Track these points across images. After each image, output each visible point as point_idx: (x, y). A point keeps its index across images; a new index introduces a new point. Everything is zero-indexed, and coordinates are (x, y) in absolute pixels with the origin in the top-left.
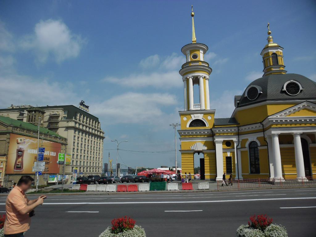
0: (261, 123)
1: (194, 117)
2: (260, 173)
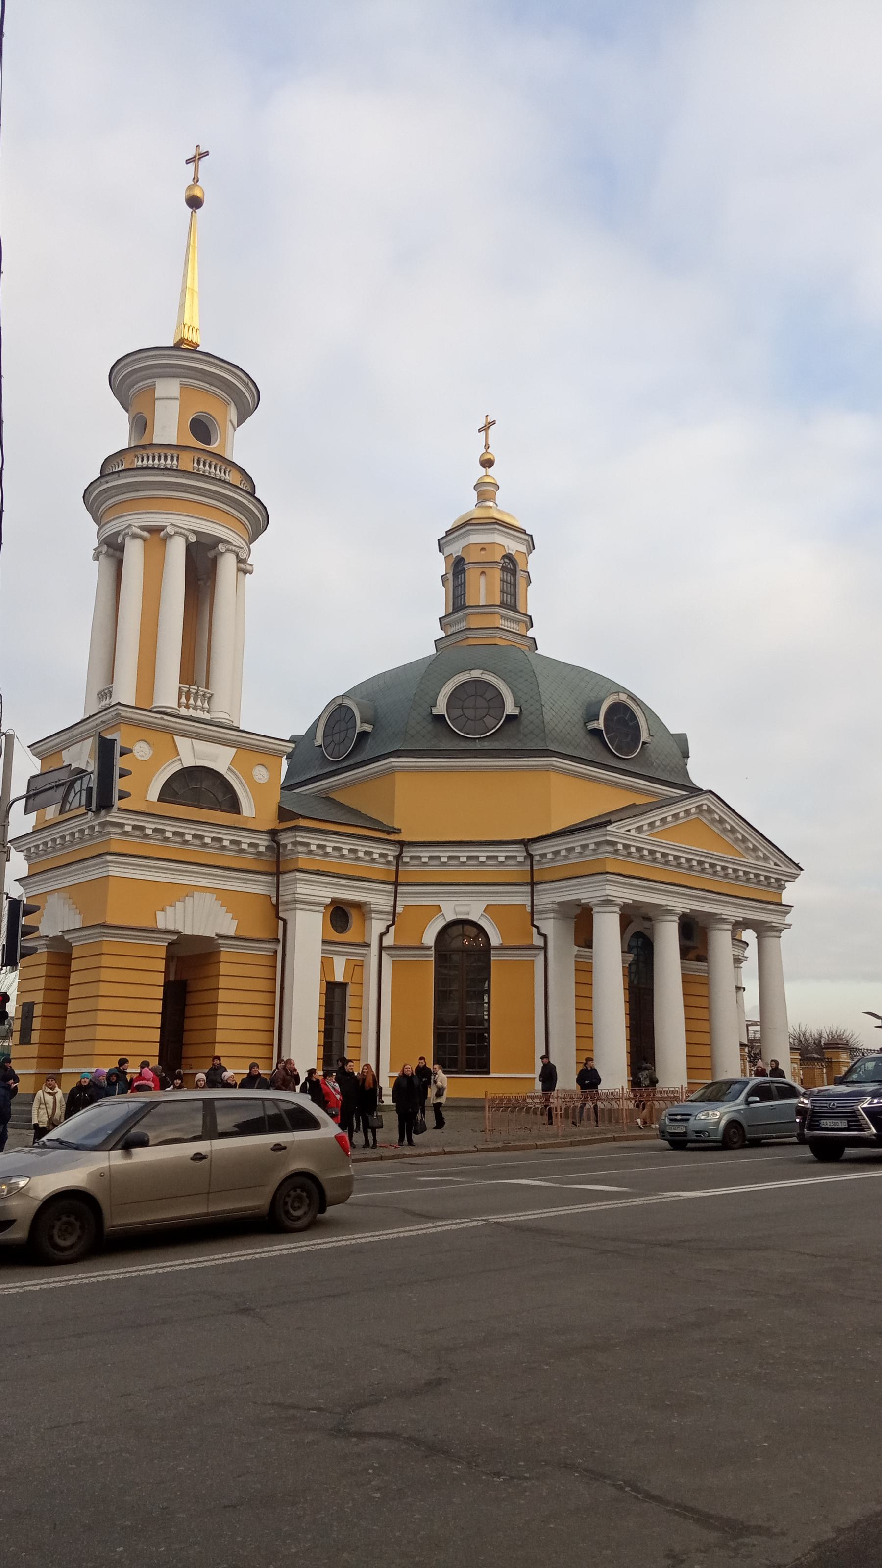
0: (526, 843)
1: (191, 753)
2: (489, 1073)
